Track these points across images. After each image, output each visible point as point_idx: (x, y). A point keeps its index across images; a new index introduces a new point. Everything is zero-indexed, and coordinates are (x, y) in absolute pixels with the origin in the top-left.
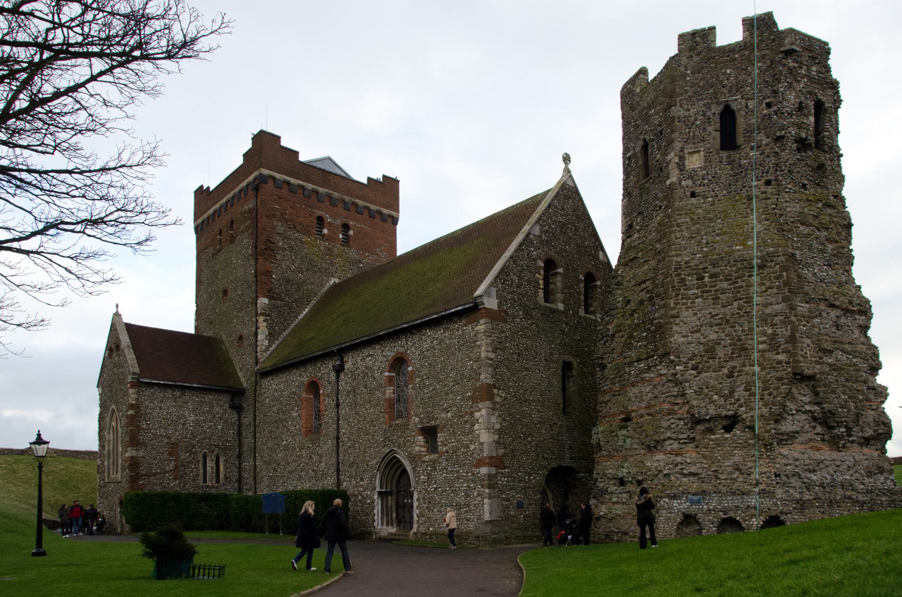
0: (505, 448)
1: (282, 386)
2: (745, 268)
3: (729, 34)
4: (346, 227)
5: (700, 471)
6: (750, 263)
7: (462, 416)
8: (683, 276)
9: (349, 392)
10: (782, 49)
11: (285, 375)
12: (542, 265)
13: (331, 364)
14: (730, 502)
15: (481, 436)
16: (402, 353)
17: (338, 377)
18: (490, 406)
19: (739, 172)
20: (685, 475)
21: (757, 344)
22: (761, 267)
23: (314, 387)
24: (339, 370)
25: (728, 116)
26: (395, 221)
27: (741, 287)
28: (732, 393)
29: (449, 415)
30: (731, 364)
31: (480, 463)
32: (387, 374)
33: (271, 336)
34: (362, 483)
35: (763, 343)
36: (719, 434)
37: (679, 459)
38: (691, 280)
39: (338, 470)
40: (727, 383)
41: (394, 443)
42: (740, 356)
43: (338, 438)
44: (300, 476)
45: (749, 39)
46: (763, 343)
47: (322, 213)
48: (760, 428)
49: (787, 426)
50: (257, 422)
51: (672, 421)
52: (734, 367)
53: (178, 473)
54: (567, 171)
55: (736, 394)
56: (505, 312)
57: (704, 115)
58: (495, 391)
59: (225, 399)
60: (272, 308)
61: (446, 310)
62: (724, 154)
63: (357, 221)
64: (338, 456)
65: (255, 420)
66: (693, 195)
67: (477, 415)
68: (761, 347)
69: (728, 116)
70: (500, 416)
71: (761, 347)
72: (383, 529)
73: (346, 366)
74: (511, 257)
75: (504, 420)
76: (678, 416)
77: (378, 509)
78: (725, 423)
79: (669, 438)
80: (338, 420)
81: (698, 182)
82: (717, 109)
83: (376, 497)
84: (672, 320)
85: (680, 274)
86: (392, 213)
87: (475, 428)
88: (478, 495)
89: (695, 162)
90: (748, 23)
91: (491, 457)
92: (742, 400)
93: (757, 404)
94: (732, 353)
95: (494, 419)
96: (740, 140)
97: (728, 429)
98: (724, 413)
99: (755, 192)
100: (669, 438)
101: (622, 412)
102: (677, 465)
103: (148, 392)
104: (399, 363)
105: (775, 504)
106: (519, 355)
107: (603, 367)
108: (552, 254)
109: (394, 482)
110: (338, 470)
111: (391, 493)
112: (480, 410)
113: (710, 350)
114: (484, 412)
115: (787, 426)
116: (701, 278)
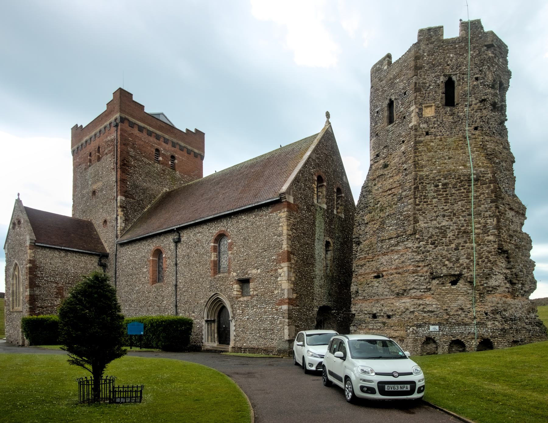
0: (297, 293)
1: (135, 252)
2: (466, 180)
3: (452, 32)
5: (435, 310)
6: (469, 178)
7: (268, 272)
8: (424, 184)
9: (184, 256)
10: (486, 43)
11: (137, 245)
12: (316, 179)
13: (171, 238)
14: (457, 330)
15: (283, 285)
16: (224, 231)
17: (176, 246)
18: (290, 265)
19: (458, 121)
20: (425, 312)
22: (477, 180)
23: (158, 253)
24: (177, 242)
27: (463, 192)
28: (458, 260)
29: (259, 271)
30: (456, 241)
31: (281, 303)
32: (212, 244)
34: (193, 314)
35: (478, 228)
36: (448, 286)
37: (421, 302)
39: (176, 306)
41: (217, 289)
42: (463, 237)
43: (176, 285)
44: (148, 310)
45: (464, 36)
46: (478, 228)
48: (477, 283)
49: (493, 282)
50: (117, 274)
51: (416, 277)
52: (459, 244)
55: (461, 261)
56: (297, 205)
57: (435, 83)
58: (292, 256)
59: (95, 260)
61: (258, 202)
62: (448, 109)
64: (176, 297)
65: (116, 273)
66: (427, 134)
67: (280, 271)
68: (477, 231)
70: (294, 272)
71: (477, 231)
72: (210, 343)
73: (182, 239)
74: (300, 171)
75: (296, 275)
76: (420, 274)
77: (205, 332)
78: (453, 279)
79: (414, 288)
80: (177, 274)
81: (431, 126)
83: (204, 323)
84: (418, 212)
85: (422, 183)
87: (279, 279)
88: (280, 323)
90: (464, 25)
91: (289, 299)
92: (465, 265)
94: (458, 235)
95: (292, 274)
97: (454, 283)
98: (453, 273)
100: (414, 288)
101: (375, 272)
102: (419, 306)
104: (220, 237)
105: (487, 332)
106: (304, 233)
107: (359, 243)
109: (216, 315)
110: (176, 306)
111: (214, 321)
112: (282, 268)
114: (285, 269)
115: (493, 282)
116: (437, 186)
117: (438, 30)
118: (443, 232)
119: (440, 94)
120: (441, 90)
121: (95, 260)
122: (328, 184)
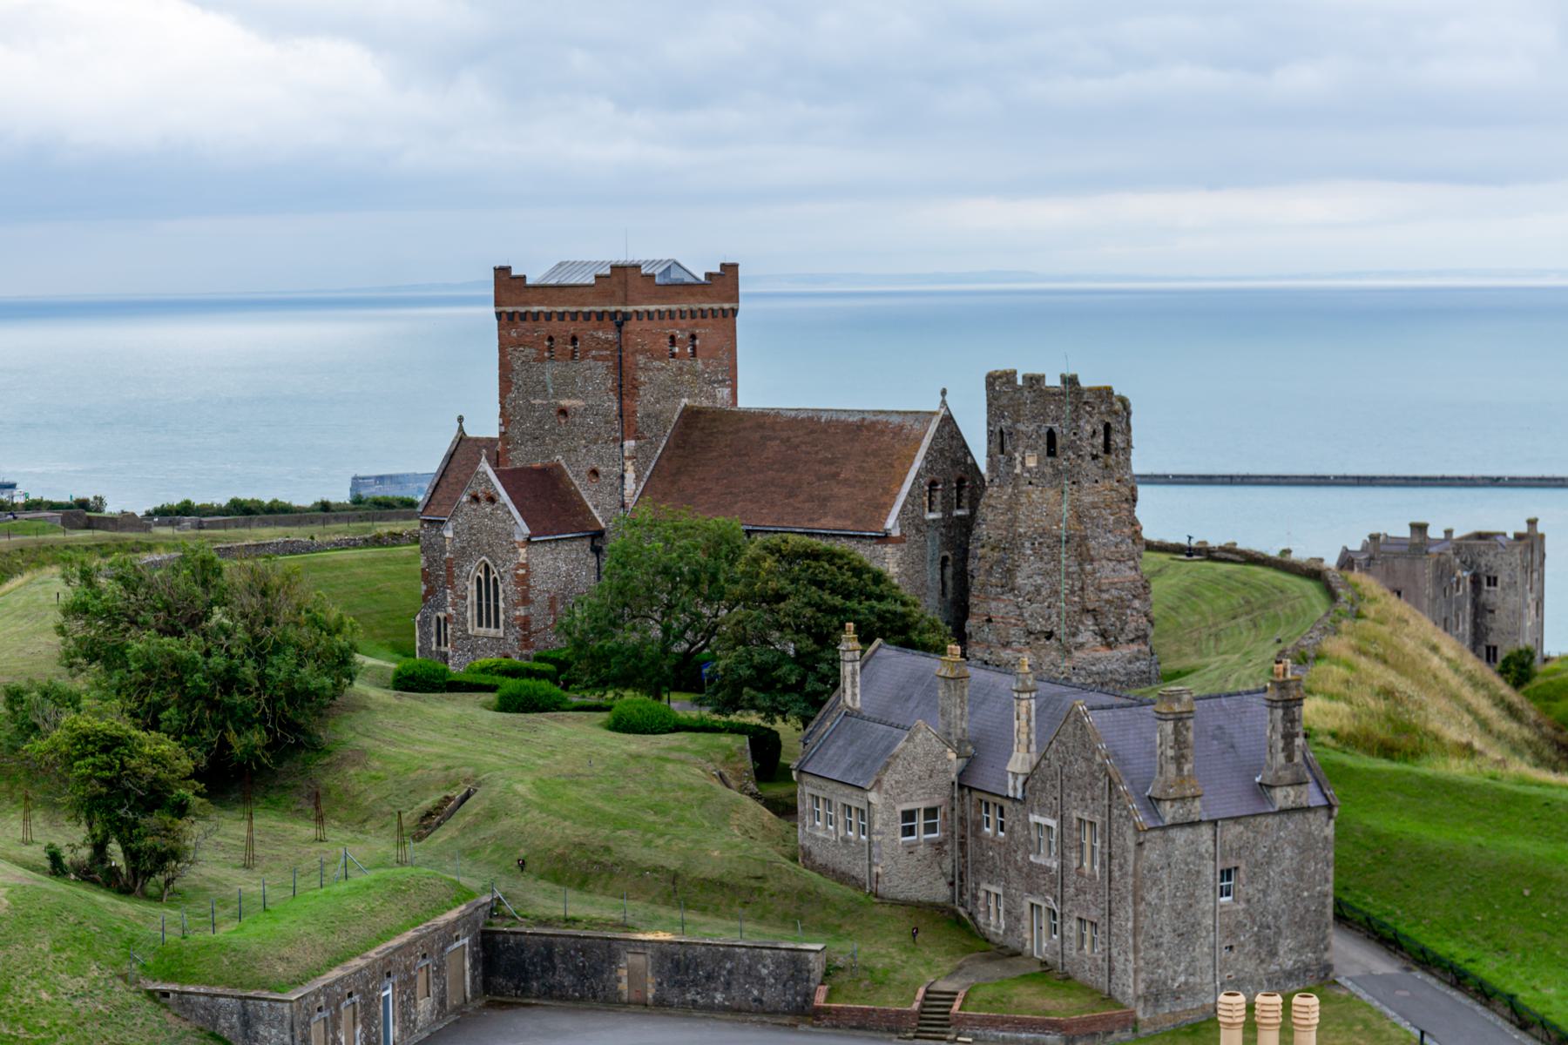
3: (1053, 381)
4: (693, 337)
21: (1064, 588)
25: (1051, 435)
26: (735, 312)
33: (638, 479)
36: (1043, 641)
38: (1027, 544)
40: (1047, 612)
47: (669, 331)
49: (1080, 639)
54: (944, 402)
60: (638, 449)
69: (1051, 435)
82: (1044, 431)
89: (1031, 463)
90: (1064, 379)
93: (1063, 626)
96: (1058, 452)
97: (1048, 638)
99: (1066, 488)
103: (533, 548)
108: (935, 476)
115: (1080, 639)
118: (1038, 590)
119: (1042, 444)
120: (1045, 439)
121: (587, 542)
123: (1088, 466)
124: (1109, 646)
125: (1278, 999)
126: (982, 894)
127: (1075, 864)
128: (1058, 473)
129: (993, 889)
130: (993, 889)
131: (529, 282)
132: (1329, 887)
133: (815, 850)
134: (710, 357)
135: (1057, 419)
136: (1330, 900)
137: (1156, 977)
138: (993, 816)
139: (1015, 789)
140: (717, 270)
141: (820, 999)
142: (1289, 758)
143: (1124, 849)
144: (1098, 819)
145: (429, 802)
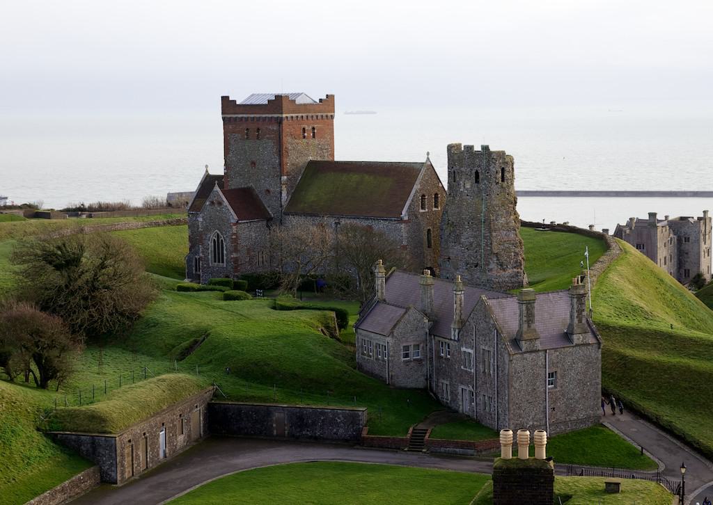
3: (478, 148)
4: (314, 128)
19: (480, 191)
25: (477, 173)
26: (332, 117)
38: (466, 223)
47: (303, 126)
49: (490, 267)
53: (250, 263)
54: (428, 159)
62: (476, 184)
63: (317, 123)
69: (477, 173)
82: (474, 171)
86: (332, 114)
89: (468, 186)
97: (476, 266)
99: (484, 198)
113: (471, 244)
115: (490, 267)
117: (472, 147)
119: (473, 176)
121: (265, 223)
122: (429, 196)
123: (494, 186)
124: (504, 270)
125: (511, 432)
126: (440, 384)
127: (482, 370)
128: (480, 191)
129: (443, 381)
130: (445, 382)
131: (237, 103)
132: (599, 381)
133: (363, 364)
134: (321, 138)
135: (479, 166)
136: (600, 386)
137: (519, 422)
138: (445, 348)
139: (455, 336)
140: (324, 97)
141: (364, 434)
142: (580, 321)
143: (504, 363)
144: (492, 349)
145: (185, 344)
